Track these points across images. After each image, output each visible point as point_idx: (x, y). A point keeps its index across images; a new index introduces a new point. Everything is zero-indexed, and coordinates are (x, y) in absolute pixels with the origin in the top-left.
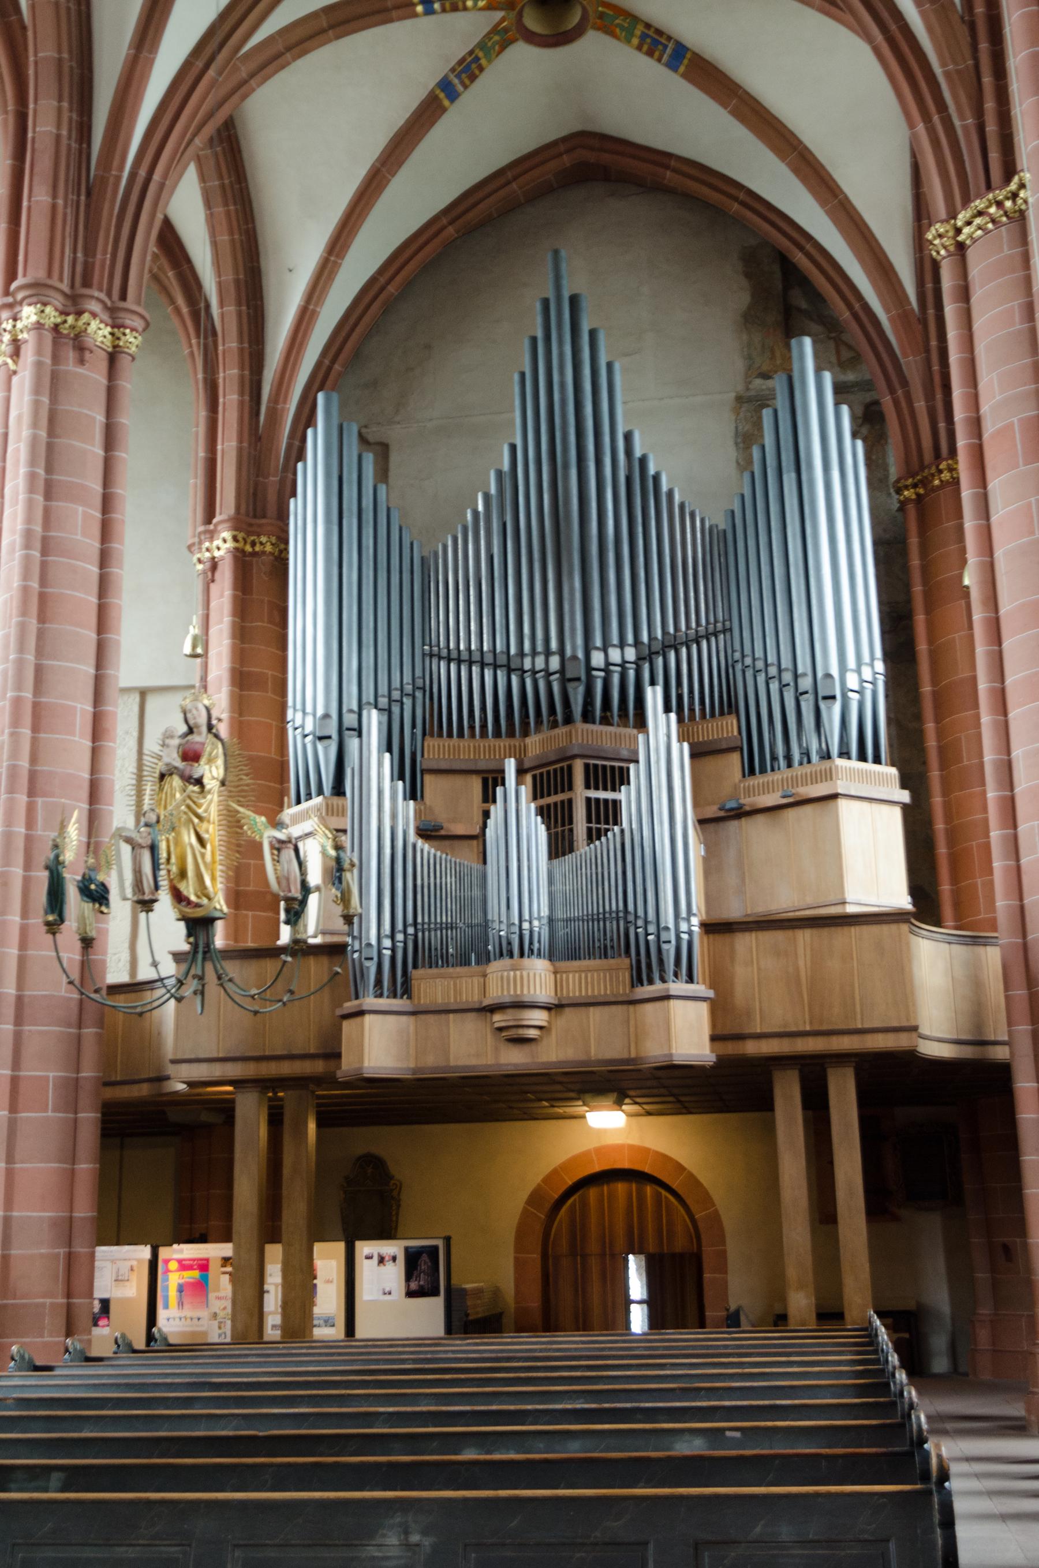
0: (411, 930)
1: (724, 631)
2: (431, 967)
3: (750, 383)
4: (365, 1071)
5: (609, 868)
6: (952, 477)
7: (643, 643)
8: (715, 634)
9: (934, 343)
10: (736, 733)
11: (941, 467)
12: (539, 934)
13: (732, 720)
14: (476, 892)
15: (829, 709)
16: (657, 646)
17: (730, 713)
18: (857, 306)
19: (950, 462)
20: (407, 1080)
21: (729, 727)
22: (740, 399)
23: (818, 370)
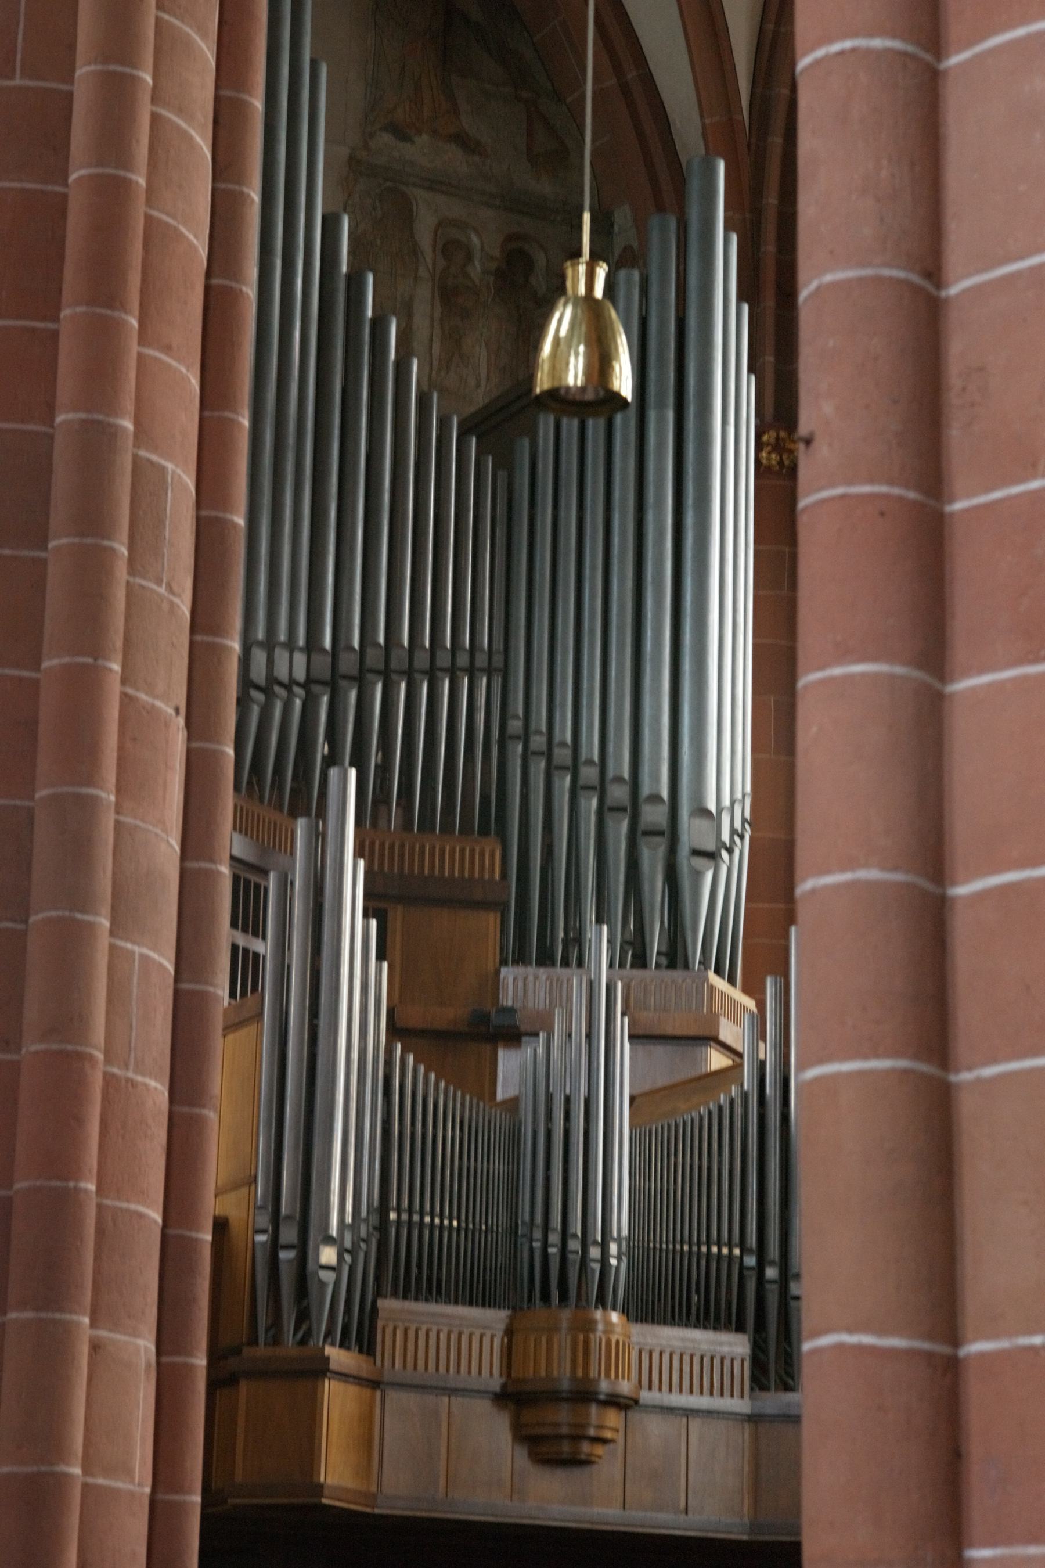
0: (375, 1220)
1: (489, 672)
2: (405, 1297)
3: (371, 136)
4: (326, 1492)
5: (720, 1163)
6: (781, 463)
7: (323, 650)
8: (472, 672)
9: (772, 200)
10: (497, 876)
11: (765, 438)
12: (618, 1268)
13: (491, 847)
14: (499, 1167)
15: (697, 876)
16: (348, 664)
17: (484, 831)
18: (631, 75)
19: (782, 434)
20: (739, 1543)
21: (486, 859)
22: (353, 161)
23: (727, 229)
